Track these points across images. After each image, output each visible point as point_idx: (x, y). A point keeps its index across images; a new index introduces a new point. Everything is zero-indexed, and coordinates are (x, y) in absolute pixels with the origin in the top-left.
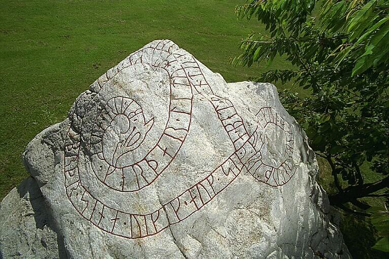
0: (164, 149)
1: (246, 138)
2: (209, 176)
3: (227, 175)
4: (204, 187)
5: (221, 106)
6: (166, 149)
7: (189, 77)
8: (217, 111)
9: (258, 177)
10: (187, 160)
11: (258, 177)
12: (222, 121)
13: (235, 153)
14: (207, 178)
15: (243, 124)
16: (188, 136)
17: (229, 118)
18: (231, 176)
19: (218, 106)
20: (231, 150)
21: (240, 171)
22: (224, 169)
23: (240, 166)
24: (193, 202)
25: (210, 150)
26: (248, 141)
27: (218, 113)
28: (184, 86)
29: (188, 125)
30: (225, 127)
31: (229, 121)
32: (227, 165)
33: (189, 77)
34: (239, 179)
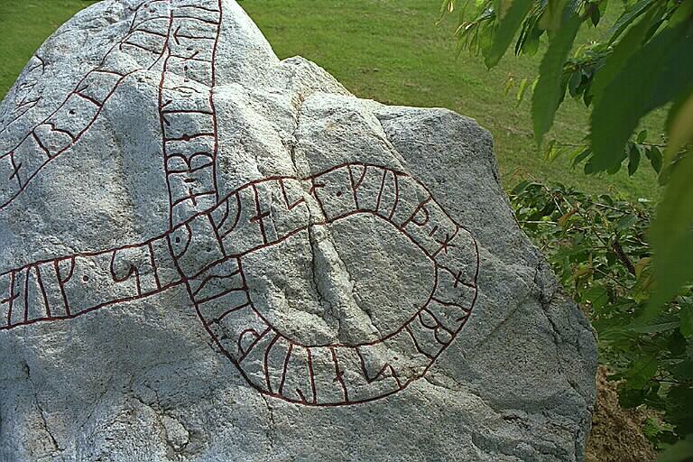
0: (17, 163)
1: (205, 202)
2: (67, 257)
3: (116, 280)
4: (39, 276)
5: (177, 99)
6: (20, 165)
7: (172, 39)
8: (161, 113)
9: (225, 337)
10: (39, 199)
11: (225, 337)
12: (165, 140)
13: (167, 234)
14: (57, 260)
15: (213, 163)
16: (69, 150)
17: (186, 138)
18: (127, 286)
19: (169, 102)
20: (158, 220)
21: (160, 289)
22: (115, 262)
23: (166, 273)
24: (7, 303)
25: (107, 202)
26: (207, 212)
27: (162, 119)
28: (145, 52)
29: (84, 128)
30: (166, 158)
31: (182, 145)
32: (131, 254)
33: (172, 39)
34: (147, 307)
